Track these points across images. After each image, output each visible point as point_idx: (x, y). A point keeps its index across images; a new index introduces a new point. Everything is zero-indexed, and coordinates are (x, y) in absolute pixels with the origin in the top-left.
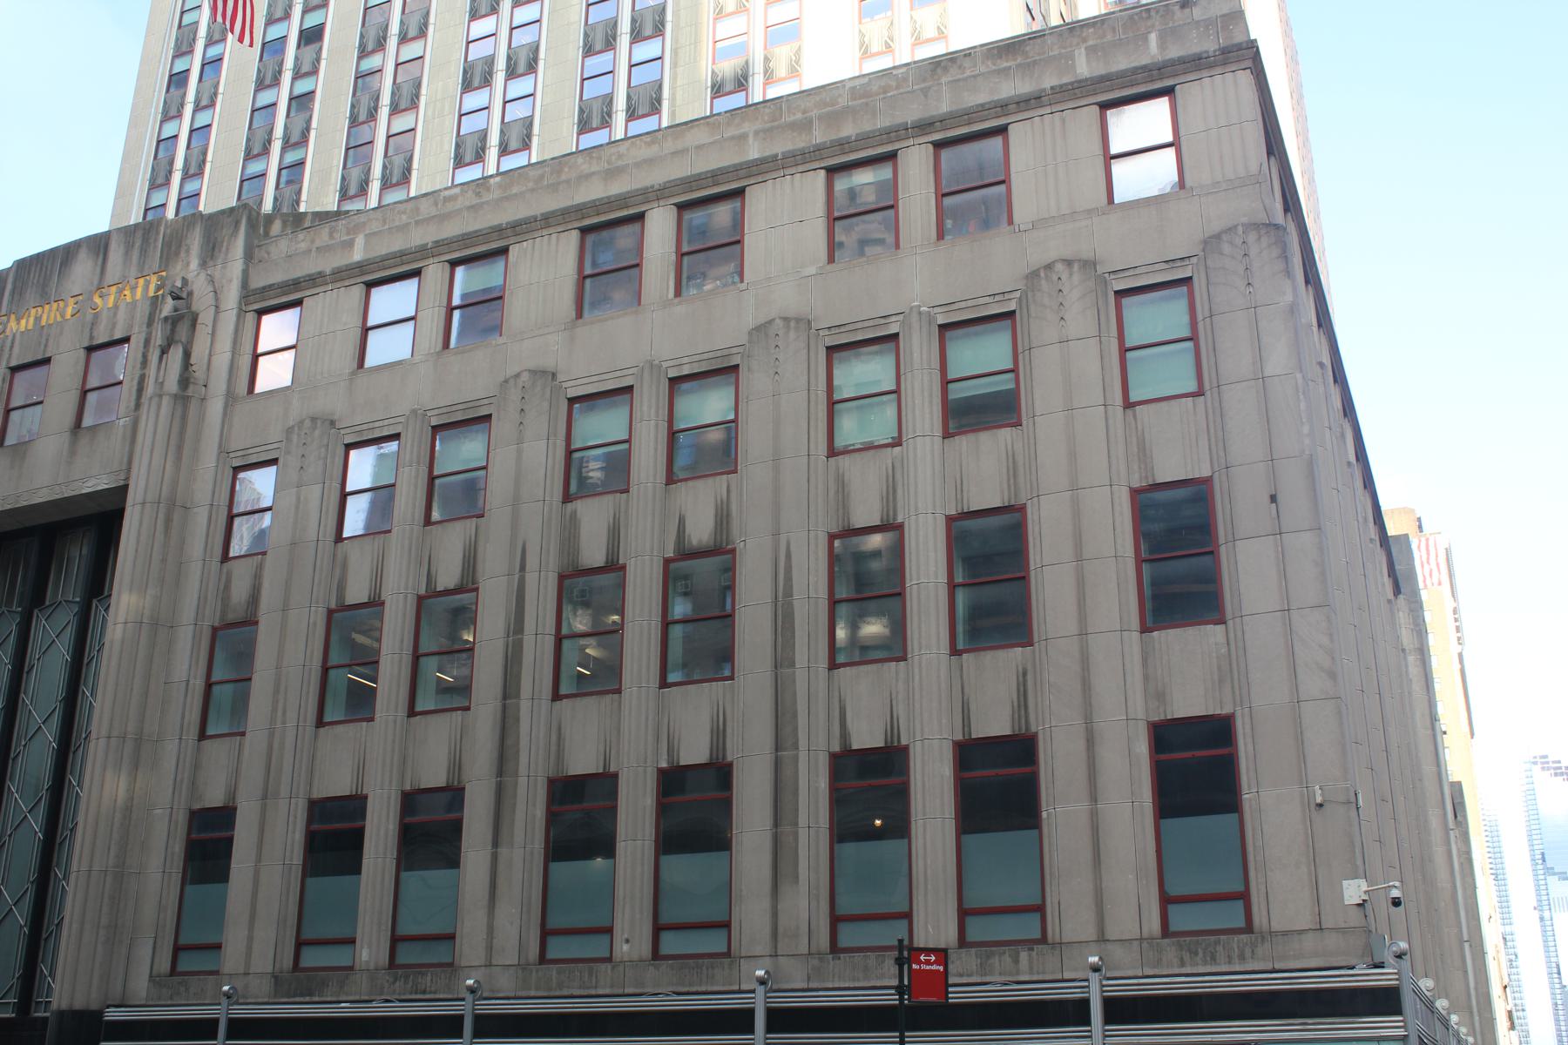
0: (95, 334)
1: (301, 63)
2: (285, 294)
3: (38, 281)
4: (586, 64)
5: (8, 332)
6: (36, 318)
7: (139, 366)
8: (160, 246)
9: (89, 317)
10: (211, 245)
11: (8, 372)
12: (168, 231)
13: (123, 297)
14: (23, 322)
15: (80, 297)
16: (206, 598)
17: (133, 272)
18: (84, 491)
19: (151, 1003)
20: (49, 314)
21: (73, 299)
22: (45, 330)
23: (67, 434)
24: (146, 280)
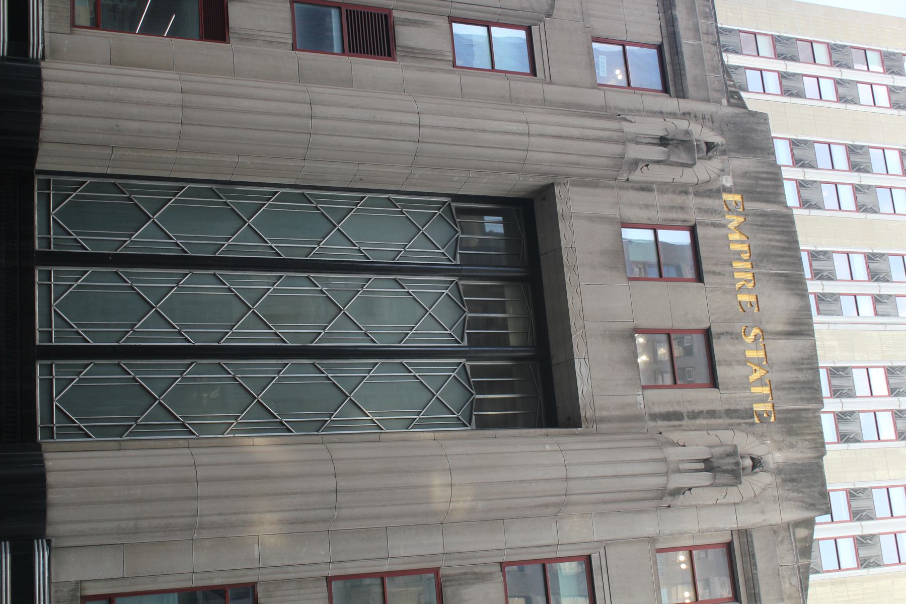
1: (864, 193)
2: (746, 581)
3: (773, 247)
4: (840, 492)
5: (729, 217)
6: (739, 253)
7: (691, 408)
8: (798, 407)
9: (740, 327)
10: (795, 476)
11: (692, 224)
12: (810, 415)
13: (754, 367)
14: (736, 236)
15: (756, 309)
16: (469, 558)
17: (776, 377)
18: (576, 361)
19: (53, 590)
20: (742, 270)
21: (753, 299)
22: (727, 268)
23: (630, 325)
24: (767, 396)
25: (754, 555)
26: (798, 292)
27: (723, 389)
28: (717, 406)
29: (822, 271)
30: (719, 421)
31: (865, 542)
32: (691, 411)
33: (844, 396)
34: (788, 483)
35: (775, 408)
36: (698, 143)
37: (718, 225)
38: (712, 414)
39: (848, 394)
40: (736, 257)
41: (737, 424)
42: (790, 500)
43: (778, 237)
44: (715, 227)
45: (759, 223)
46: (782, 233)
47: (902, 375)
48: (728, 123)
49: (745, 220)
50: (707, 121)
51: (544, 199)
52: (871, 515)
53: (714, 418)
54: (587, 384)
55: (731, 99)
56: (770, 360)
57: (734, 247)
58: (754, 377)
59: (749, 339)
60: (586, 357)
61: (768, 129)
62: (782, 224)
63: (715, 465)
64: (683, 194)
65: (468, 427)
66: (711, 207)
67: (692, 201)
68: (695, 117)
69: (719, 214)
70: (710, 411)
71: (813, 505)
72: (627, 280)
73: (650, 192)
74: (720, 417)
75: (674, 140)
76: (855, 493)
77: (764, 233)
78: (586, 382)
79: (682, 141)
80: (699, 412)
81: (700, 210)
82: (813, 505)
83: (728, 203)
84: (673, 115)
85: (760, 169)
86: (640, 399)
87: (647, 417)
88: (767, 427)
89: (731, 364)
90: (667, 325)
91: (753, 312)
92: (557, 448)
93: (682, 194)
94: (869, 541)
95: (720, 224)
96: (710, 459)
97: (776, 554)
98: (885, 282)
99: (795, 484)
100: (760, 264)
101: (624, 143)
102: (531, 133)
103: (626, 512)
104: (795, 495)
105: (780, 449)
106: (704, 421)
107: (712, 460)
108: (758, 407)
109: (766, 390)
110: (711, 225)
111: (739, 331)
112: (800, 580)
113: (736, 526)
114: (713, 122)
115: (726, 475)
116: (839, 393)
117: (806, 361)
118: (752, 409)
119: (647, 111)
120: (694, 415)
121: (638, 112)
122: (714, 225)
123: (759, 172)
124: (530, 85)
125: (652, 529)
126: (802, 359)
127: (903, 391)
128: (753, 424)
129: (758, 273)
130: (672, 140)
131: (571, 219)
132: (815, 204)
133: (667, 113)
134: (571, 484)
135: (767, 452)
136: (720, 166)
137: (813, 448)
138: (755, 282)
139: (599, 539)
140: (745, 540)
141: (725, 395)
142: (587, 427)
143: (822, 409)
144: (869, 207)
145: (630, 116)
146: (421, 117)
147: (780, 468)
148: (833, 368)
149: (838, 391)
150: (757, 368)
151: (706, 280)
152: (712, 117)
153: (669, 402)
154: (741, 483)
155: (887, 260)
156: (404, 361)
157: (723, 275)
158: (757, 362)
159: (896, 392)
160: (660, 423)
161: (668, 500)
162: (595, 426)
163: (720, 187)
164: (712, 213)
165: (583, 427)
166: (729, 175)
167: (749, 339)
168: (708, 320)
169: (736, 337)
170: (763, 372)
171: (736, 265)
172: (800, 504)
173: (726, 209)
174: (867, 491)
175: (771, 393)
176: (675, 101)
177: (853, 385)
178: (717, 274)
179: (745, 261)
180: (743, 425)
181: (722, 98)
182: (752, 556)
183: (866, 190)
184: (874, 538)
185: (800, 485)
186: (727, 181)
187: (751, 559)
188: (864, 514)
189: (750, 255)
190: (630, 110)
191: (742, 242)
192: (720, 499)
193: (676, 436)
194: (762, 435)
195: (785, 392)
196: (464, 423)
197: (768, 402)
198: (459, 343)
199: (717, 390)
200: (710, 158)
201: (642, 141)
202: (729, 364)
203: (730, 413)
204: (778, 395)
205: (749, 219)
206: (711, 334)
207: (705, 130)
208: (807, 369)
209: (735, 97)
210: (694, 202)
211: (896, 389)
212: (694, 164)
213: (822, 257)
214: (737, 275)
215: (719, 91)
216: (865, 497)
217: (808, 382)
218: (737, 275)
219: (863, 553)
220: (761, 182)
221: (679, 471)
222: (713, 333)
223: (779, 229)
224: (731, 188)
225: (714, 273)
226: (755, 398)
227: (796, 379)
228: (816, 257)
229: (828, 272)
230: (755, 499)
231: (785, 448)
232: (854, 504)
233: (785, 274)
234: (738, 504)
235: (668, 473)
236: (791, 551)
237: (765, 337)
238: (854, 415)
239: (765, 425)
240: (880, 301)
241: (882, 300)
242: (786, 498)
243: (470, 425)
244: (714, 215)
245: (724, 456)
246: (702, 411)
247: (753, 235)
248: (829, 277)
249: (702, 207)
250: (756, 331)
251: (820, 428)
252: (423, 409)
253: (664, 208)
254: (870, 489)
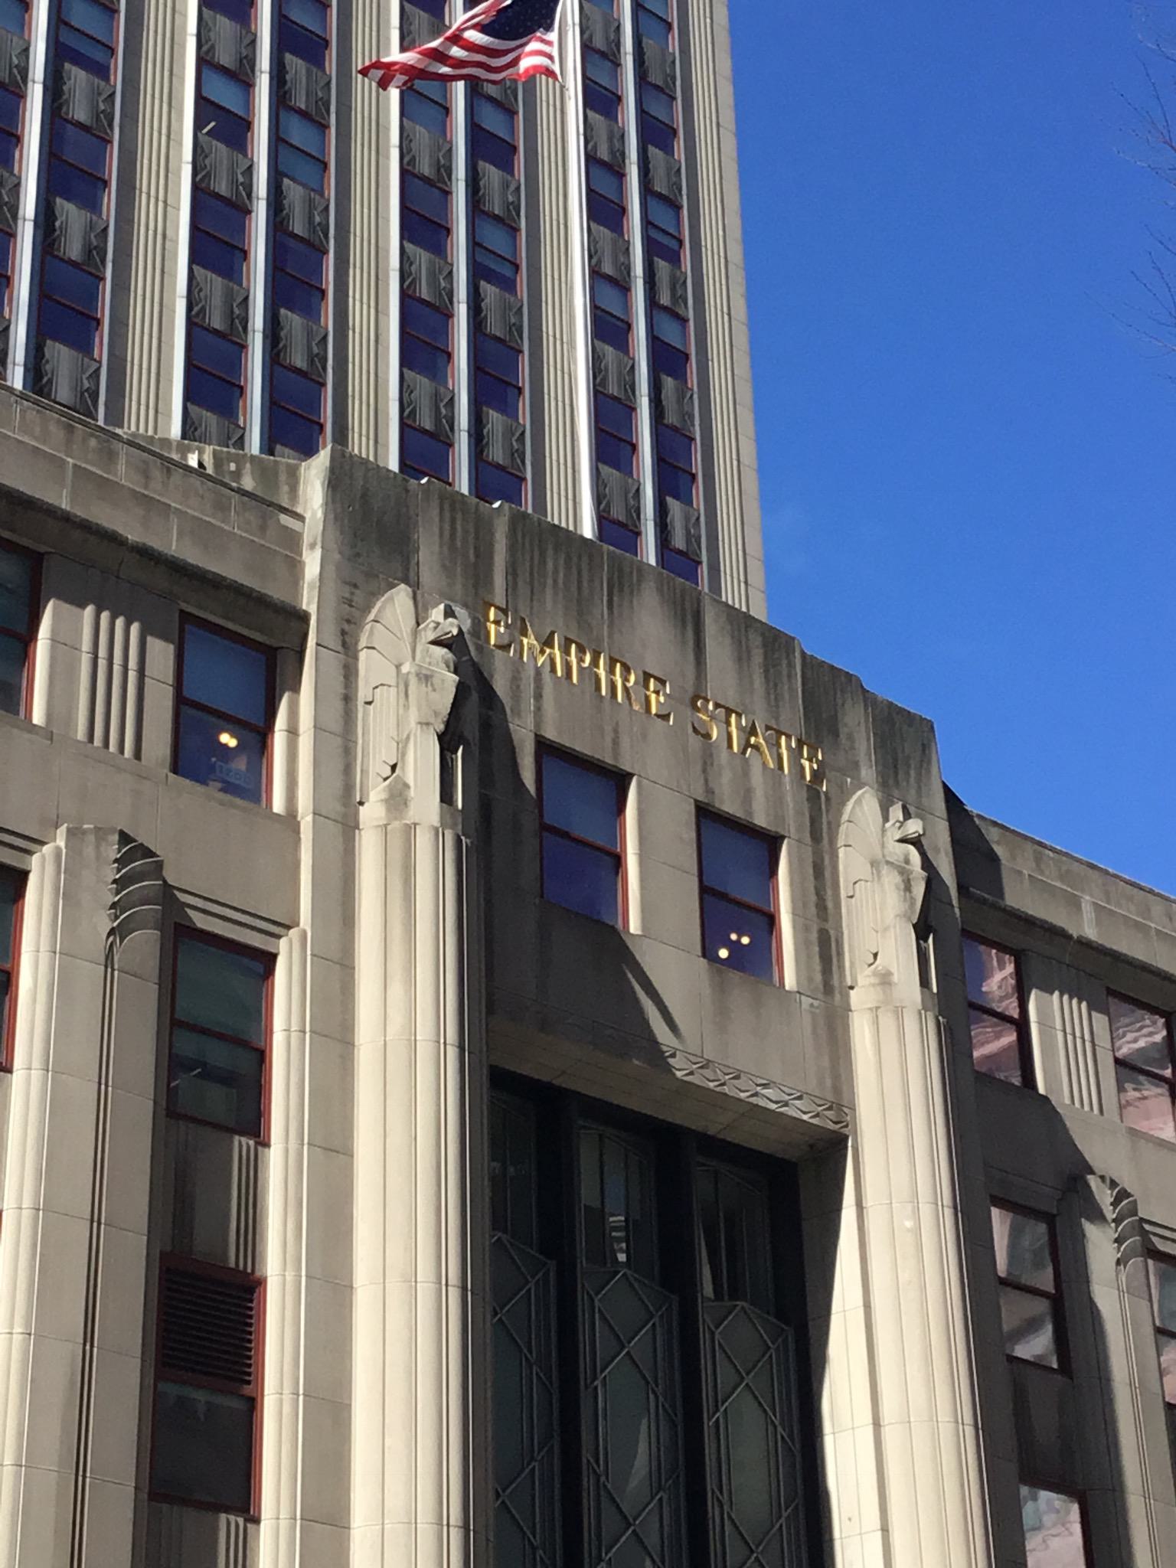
30: (827, 861)
85: (436, 530)
120: (821, 907)
122: (538, 696)
128: (826, 793)
151: (629, 770)
152: (346, 583)
160: (835, 982)
162: (845, 1110)
164: (518, 687)
180: (830, 817)
195: (781, 704)
202: (747, 795)
203: (816, 836)
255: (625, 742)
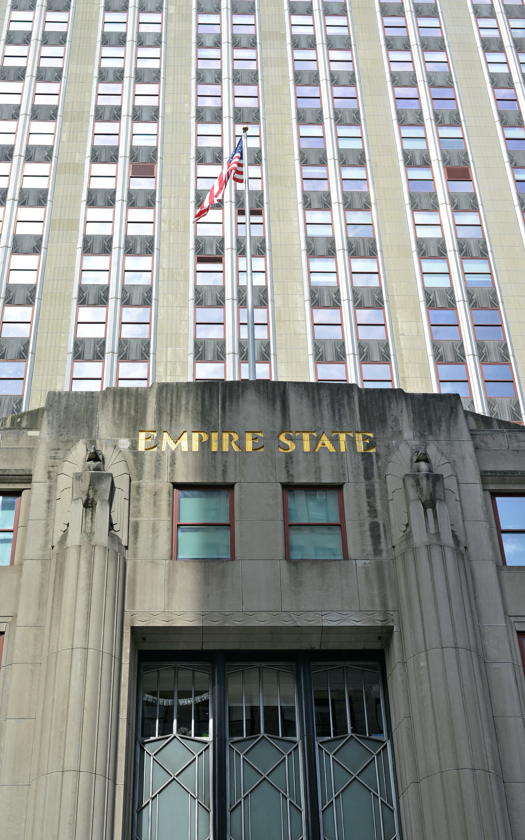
0: (294, 472)
1: (14, 296)
5: (164, 449)
6: (202, 444)
7: (366, 514)
8: (357, 409)
11: (171, 485)
13: (320, 445)
14: (184, 442)
15: (260, 434)
18: (325, 624)
21: (249, 436)
22: (219, 457)
23: (284, 563)
25: (505, 472)
26: (240, 390)
27: (345, 478)
28: (362, 487)
29: (95, 352)
30: (377, 487)
31: (365, 354)
32: (369, 514)
33: (224, 350)
34: (433, 430)
35: (360, 430)
36: (92, 469)
37: (173, 460)
38: (370, 493)
39: (222, 346)
40: (206, 447)
41: (379, 470)
42: (449, 430)
43: (183, 402)
44: (175, 463)
45: (169, 418)
46: (179, 398)
47: (204, 292)
48: (59, 434)
49: (166, 432)
50: (58, 455)
51: (144, 639)
52: (341, 344)
53: (374, 491)
54: (348, 615)
55: (22, 425)
56: (311, 428)
57: (196, 447)
58: (328, 445)
59: (292, 446)
60: (320, 613)
61: (66, 394)
62: (169, 395)
63: (429, 498)
64: (140, 491)
65: (386, 745)
66: (154, 464)
67: (147, 483)
68: (53, 466)
69: (160, 457)
70: (367, 495)
71: (452, 409)
72: (234, 562)
73: (139, 525)
74: (373, 486)
75: (88, 493)
76: (320, 355)
77: (180, 415)
78: (346, 616)
79: (90, 485)
80: (369, 505)
81: (157, 476)
82: (452, 409)
83: (148, 447)
84: (51, 490)
85: (111, 408)
86: (360, 563)
87: (378, 558)
88: (380, 441)
89: (319, 468)
90: (280, 525)
91: (263, 438)
92: (423, 655)
93: (139, 492)
94: (365, 350)
95: (171, 457)
96: (423, 501)
97: (499, 450)
98: (108, 292)
99: (433, 423)
100: (213, 424)
101: (94, 546)
102: (84, 647)
103: (475, 591)
104: (443, 424)
105: (400, 433)
106: (378, 503)
107: (423, 500)
108: (360, 447)
109: (343, 437)
110: (173, 467)
111: (284, 455)
112: (520, 431)
113: (478, 485)
114: (58, 449)
115: (437, 488)
116: (221, 355)
117: (311, 394)
118: (363, 454)
119: (48, 516)
120: (373, 511)
121: (48, 526)
122: (173, 463)
123: (114, 410)
124: (17, 641)
125: (489, 568)
126: (309, 397)
127: (220, 294)
128: (377, 454)
129: (222, 427)
130: (88, 495)
131: (171, 613)
132: (24, 346)
133: (50, 495)
134: (460, 644)
135: (407, 445)
136: (111, 449)
137: (397, 401)
138: (232, 432)
139: (504, 622)
140: (489, 478)
141: (351, 477)
142: (393, 621)
143: (358, 386)
144: (29, 294)
145: (55, 536)
146: (68, 769)
147: (419, 435)
148: (195, 355)
149: (218, 355)
150: (321, 442)
152: (52, 450)
153: (362, 534)
154: (442, 475)
155: (87, 286)
156: (320, 809)
157: (226, 462)
158: (315, 442)
159: (221, 301)
160: (383, 546)
161: (462, 548)
162: (391, 613)
163: (132, 452)
164: (160, 464)
165: (392, 625)
166: (117, 441)
167: (292, 446)
168: (275, 484)
169: (290, 458)
170: (324, 438)
171: (215, 448)
172: (452, 421)
173: (155, 449)
174: (317, 344)
175: (345, 432)
176: (35, 486)
177: (213, 340)
178: (226, 468)
179: (210, 438)
180: (379, 464)
181: (27, 435)
182: (504, 473)
183: (11, 294)
184: (362, 345)
185: (434, 418)
186: (124, 443)
187: (508, 475)
188: (339, 350)
189: (203, 432)
190: (47, 534)
191: (190, 439)
192: (455, 497)
193: (397, 534)
194: (388, 447)
196: (383, 749)
197: (354, 437)
198: (298, 746)
199: (345, 486)
200: (103, 458)
201: (89, 528)
202: (318, 470)
203: (368, 475)
204: (346, 426)
205: (165, 427)
206: (288, 483)
207: (70, 458)
208: (319, 395)
209: (19, 420)
210: (149, 481)
211: (218, 301)
212: (111, 475)
213: (80, 349)
214: (226, 448)
215: (18, 437)
216: (323, 347)
217: (332, 395)
218: (226, 448)
219: (376, 357)
220: (125, 410)
221: (438, 534)
222: (288, 481)
223: (174, 399)
224: (132, 441)
225: (224, 471)
226: (352, 448)
227: (329, 406)
228: (80, 354)
229: (96, 345)
230: (453, 464)
231: (398, 427)
232: (330, 358)
233: (222, 401)
234: (457, 480)
235: (441, 546)
236: (494, 436)
237: (288, 430)
238: (243, 344)
239: (378, 443)
240: (129, 300)
241: (128, 298)
242: (447, 433)
243: (384, 742)
244: (162, 463)
245: (418, 488)
246: (368, 502)
247: (182, 426)
248: (101, 345)
249: (154, 473)
250: (282, 438)
251: (376, 390)
252: (371, 791)
253: (156, 513)
254: (315, 341)
255: (231, 469)
